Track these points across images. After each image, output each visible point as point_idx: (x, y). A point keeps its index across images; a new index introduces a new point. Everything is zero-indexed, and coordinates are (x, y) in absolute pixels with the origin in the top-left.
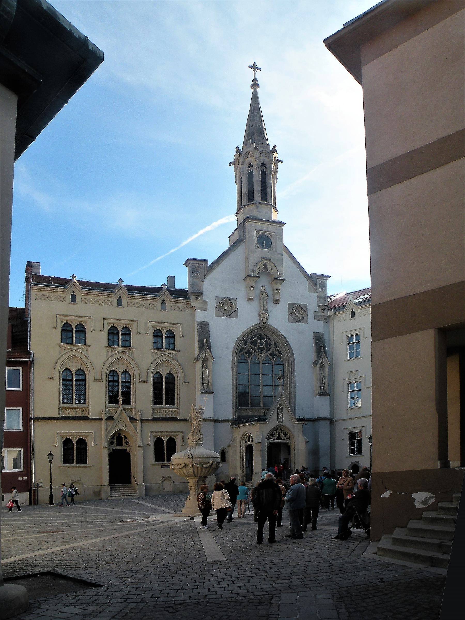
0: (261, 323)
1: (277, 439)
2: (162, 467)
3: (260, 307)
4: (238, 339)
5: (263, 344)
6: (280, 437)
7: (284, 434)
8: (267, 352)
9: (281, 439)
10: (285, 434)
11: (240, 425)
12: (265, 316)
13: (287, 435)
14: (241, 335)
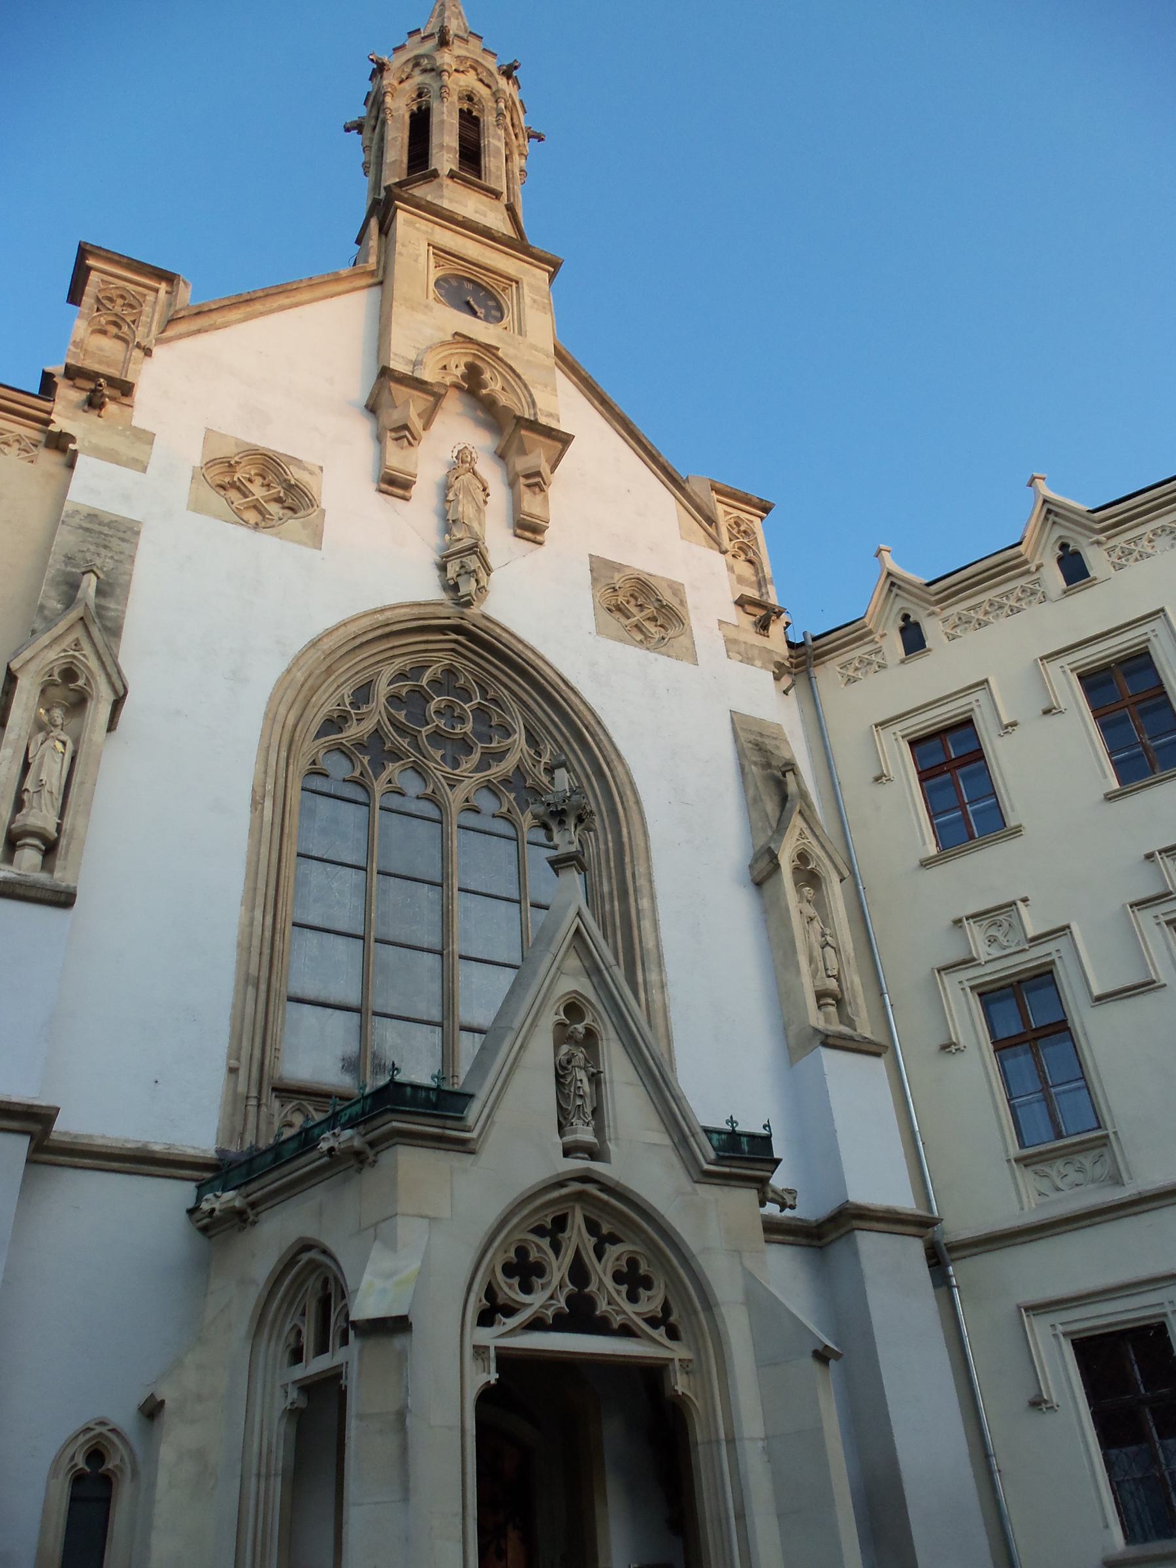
0: (449, 603)
1: (561, 1324)
3: (448, 523)
4: (314, 644)
6: (591, 1302)
7: (618, 1278)
9: (601, 1327)
11: (257, 1190)
12: (473, 563)
14: (329, 633)
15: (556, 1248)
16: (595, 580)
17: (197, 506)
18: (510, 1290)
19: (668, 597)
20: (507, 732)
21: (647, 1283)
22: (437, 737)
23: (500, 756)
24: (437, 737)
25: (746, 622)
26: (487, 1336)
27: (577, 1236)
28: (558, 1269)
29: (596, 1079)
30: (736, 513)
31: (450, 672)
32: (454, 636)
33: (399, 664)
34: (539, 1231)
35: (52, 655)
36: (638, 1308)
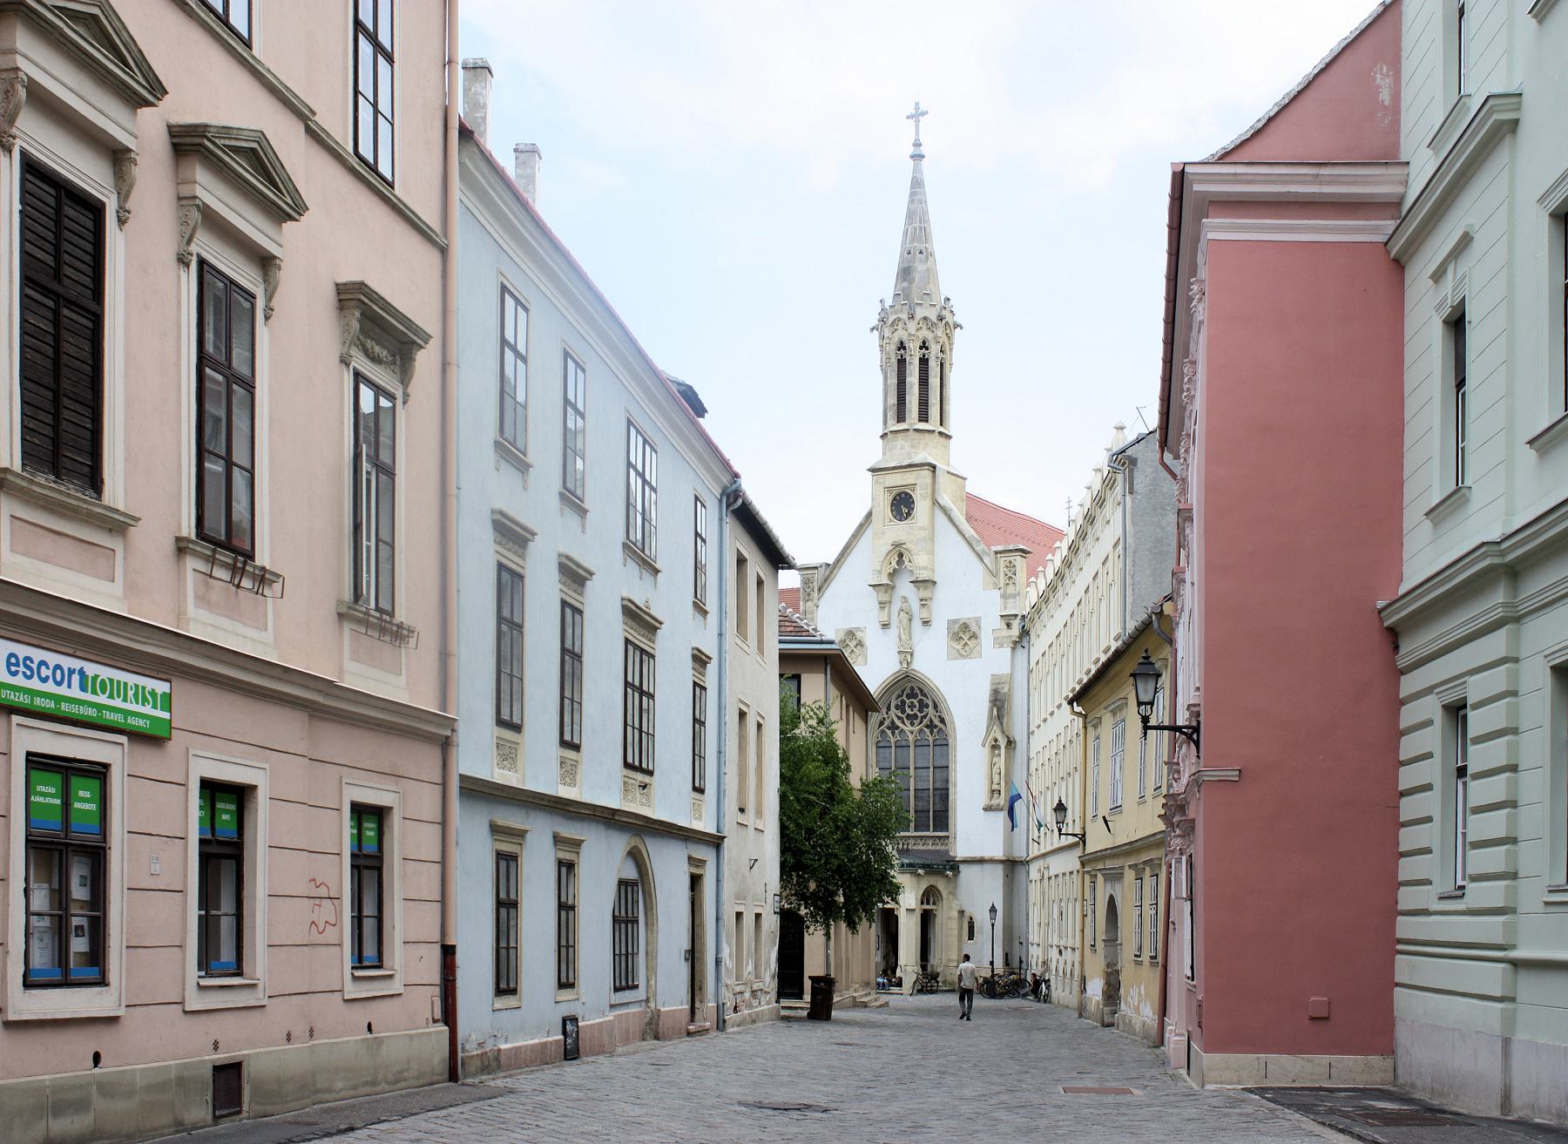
5: (912, 703)
16: (948, 632)
19: (974, 628)
20: (927, 706)
22: (908, 717)
23: (925, 717)
24: (908, 717)
30: (1008, 559)
31: (912, 689)
33: (896, 693)
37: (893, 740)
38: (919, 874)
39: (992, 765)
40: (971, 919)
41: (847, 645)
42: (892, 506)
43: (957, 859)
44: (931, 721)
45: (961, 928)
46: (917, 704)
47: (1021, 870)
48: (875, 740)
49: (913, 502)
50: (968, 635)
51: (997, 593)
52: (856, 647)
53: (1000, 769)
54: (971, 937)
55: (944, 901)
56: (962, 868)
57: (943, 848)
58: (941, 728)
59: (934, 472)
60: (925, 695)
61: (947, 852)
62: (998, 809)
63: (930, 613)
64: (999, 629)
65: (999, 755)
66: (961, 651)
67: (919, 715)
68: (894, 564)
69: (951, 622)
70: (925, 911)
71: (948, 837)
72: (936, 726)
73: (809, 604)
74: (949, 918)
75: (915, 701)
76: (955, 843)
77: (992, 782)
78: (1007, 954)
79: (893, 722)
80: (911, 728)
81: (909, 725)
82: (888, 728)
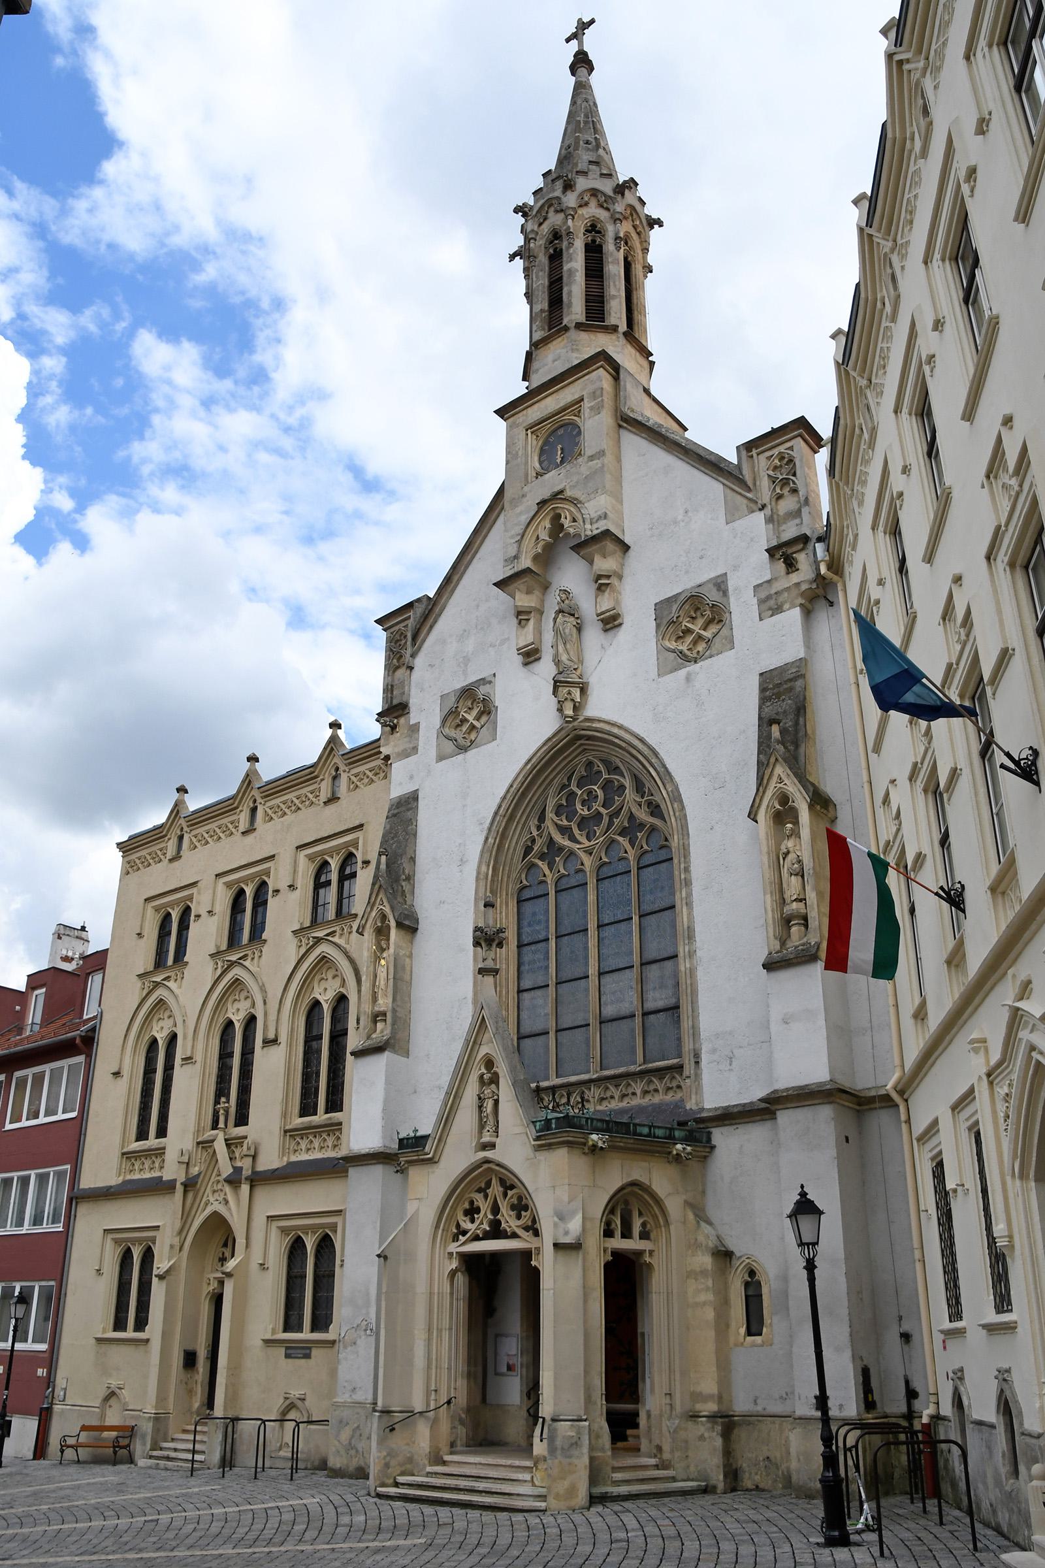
1: (487, 1236)
2: (287, 1356)
5: (590, 792)
6: (499, 1222)
7: (513, 1207)
8: (563, 830)
10: (521, 1207)
13: (526, 1208)
14: (504, 798)
15: (486, 1197)
16: (658, 626)
17: (441, 758)
18: (467, 1225)
19: (713, 596)
21: (526, 1208)
22: (583, 823)
23: (617, 813)
24: (583, 823)
25: (781, 566)
26: (453, 1247)
27: (496, 1189)
28: (485, 1206)
29: (496, 1102)
30: (776, 451)
32: (579, 742)
34: (479, 1190)
35: (373, 914)
36: (520, 1223)
37: (550, 878)
38: (595, 1146)
39: (779, 858)
40: (752, 1273)
41: (464, 720)
42: (540, 456)
43: (704, 1115)
44: (632, 817)
45: (723, 1303)
46: (600, 793)
47: (881, 1119)
48: (513, 887)
49: (579, 433)
50: (700, 622)
51: (760, 517)
52: (478, 718)
53: (799, 861)
54: (754, 1325)
55: (672, 1228)
56: (721, 1137)
57: (669, 1097)
58: (653, 829)
59: (616, 378)
60: (616, 770)
61: (679, 1105)
62: (806, 957)
63: (617, 602)
64: (769, 582)
65: (795, 833)
66: (688, 653)
67: (603, 811)
68: (544, 536)
69: (661, 607)
70: (616, 1254)
71: (681, 1067)
72: (642, 825)
73: (401, 673)
74: (691, 1274)
75: (595, 788)
76: (698, 1076)
77: (783, 902)
78: (866, 1373)
79: (551, 842)
80: (587, 844)
81: (583, 839)
82: (542, 857)
